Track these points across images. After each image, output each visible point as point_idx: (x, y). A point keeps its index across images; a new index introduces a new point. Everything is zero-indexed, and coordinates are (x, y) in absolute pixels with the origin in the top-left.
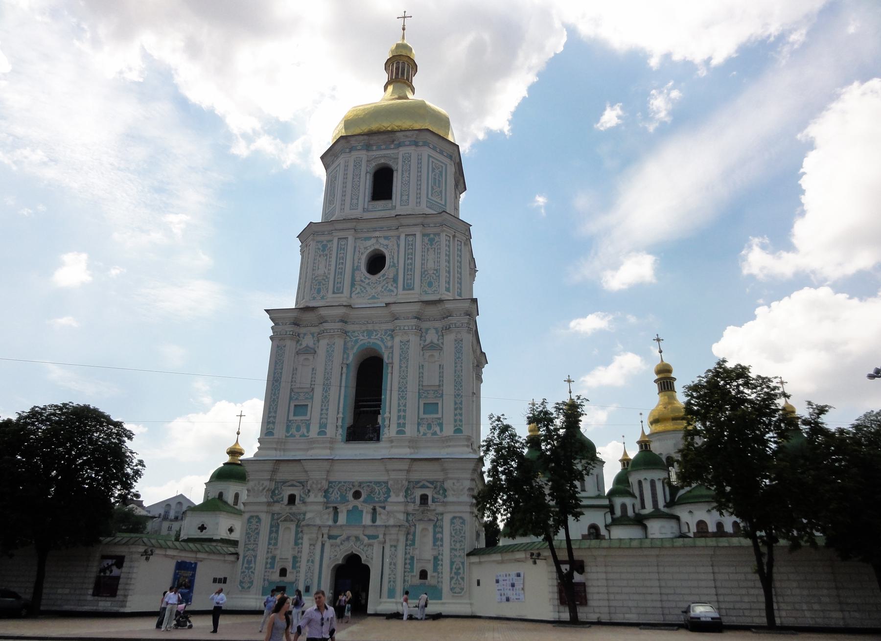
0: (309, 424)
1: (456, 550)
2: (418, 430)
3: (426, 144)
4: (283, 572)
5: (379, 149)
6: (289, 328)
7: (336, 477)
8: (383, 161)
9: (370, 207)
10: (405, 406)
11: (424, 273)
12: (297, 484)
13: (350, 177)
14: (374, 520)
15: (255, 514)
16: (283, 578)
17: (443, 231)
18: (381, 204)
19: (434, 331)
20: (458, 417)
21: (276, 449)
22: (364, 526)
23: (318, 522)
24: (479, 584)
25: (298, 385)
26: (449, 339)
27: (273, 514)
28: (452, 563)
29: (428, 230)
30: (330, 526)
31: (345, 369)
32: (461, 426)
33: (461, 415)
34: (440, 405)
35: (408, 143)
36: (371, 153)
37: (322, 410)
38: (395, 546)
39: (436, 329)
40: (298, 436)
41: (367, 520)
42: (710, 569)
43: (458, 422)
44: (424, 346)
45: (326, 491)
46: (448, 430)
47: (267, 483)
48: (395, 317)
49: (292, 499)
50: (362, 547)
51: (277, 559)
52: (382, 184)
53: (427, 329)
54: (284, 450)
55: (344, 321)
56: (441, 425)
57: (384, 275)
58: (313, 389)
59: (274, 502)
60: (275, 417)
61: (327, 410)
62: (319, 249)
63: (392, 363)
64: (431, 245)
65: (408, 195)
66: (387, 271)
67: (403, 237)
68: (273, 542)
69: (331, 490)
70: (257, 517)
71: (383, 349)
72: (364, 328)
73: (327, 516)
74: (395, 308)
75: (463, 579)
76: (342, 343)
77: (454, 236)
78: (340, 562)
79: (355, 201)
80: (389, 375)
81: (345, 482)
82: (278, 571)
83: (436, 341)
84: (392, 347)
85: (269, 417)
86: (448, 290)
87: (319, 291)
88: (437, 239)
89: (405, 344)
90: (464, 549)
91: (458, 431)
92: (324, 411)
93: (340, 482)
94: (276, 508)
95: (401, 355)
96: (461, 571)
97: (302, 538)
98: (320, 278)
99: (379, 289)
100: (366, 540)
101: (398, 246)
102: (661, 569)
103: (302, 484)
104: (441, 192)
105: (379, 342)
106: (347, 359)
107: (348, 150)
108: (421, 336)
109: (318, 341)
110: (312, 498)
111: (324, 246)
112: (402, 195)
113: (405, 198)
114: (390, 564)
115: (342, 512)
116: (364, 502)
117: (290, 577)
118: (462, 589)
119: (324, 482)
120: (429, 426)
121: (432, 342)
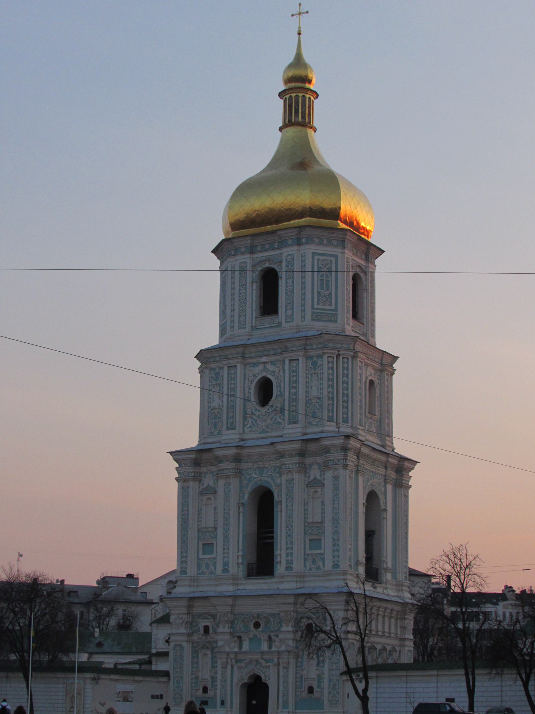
0: (216, 562)
1: (333, 670)
2: (305, 566)
3: (310, 240)
4: (205, 690)
6: (190, 469)
8: (267, 265)
10: (292, 544)
11: (308, 401)
12: (210, 617)
13: (237, 287)
14: (270, 647)
15: (178, 643)
16: (205, 694)
17: (324, 353)
18: (269, 320)
19: (316, 467)
20: (336, 553)
21: (190, 586)
22: (262, 653)
23: (227, 649)
24: (348, 698)
25: (204, 526)
26: (329, 475)
27: (193, 643)
28: (330, 681)
29: (312, 353)
30: (236, 653)
31: (241, 509)
32: (338, 561)
33: (338, 551)
34: (323, 541)
35: (289, 242)
36: (256, 256)
37: (224, 549)
39: (318, 464)
40: (207, 573)
41: (265, 647)
42: (435, 684)
43: (336, 559)
44: (309, 483)
45: (232, 622)
46: (328, 566)
47: (184, 616)
48: (281, 455)
49: (206, 629)
50: (261, 669)
51: (200, 679)
53: (311, 465)
54: (197, 586)
56: (323, 560)
57: (272, 406)
58: (216, 529)
59: (193, 633)
60: (186, 557)
61: (228, 548)
62: (212, 377)
63: (281, 502)
64: (315, 369)
65: (292, 309)
66: (275, 400)
67: (287, 362)
68: (195, 665)
69: (236, 622)
70: (180, 645)
71: (274, 487)
72: (256, 466)
73: (233, 644)
74: (279, 447)
75: (338, 693)
76: (238, 483)
77: (338, 356)
78: (246, 681)
79: (242, 319)
80: (279, 513)
81: (247, 614)
82: (201, 689)
83: (318, 477)
84: (280, 485)
85: (182, 557)
86: (330, 419)
87: (215, 425)
88: (319, 363)
89: (290, 481)
90: (339, 669)
91: (336, 566)
92: (226, 551)
93: (243, 614)
94: (195, 638)
95: (287, 494)
96: (337, 687)
97: (217, 663)
98: (216, 411)
99: (269, 421)
100: (264, 663)
101: (284, 372)
102: (409, 685)
103: (214, 617)
104: (330, 294)
105: (270, 480)
106: (243, 497)
108: (306, 472)
109: (217, 480)
110: (221, 630)
111: (217, 374)
112: (286, 309)
113: (289, 312)
114: (284, 682)
115: (245, 640)
116: (262, 631)
117: (210, 693)
118: (338, 701)
119: (230, 615)
120: (314, 562)
121: (315, 479)
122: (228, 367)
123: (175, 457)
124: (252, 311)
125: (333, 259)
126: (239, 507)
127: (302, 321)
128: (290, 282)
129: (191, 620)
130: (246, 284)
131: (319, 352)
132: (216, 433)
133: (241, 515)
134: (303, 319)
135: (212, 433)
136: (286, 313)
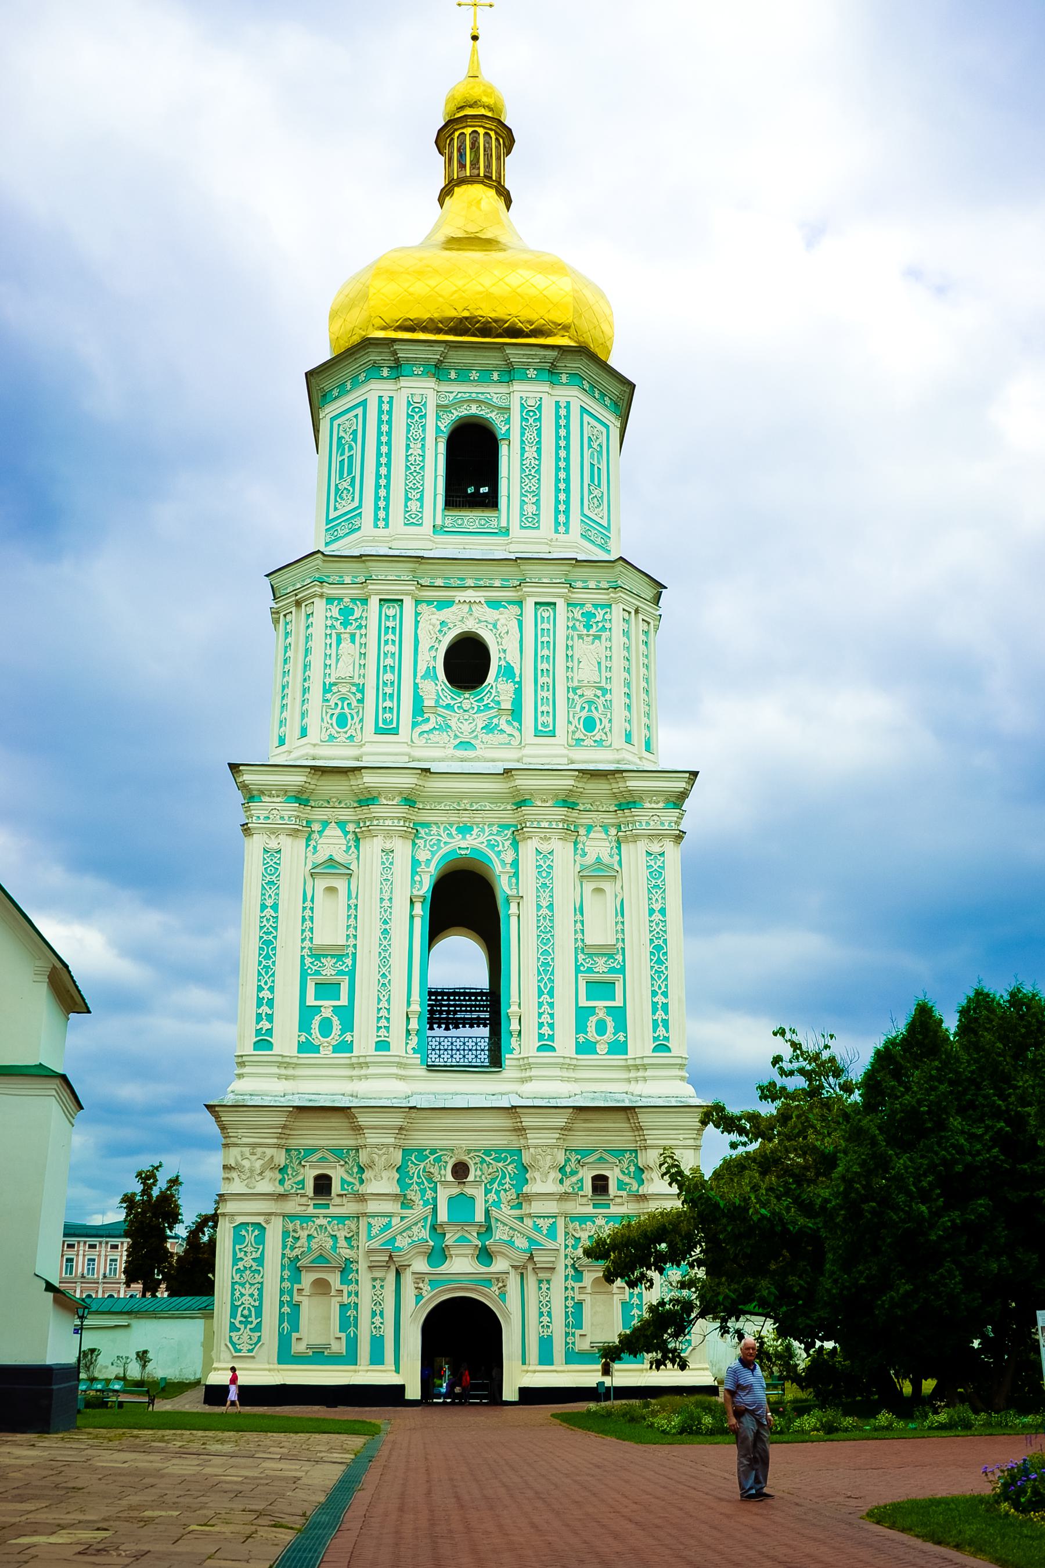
5: (463, 375)
7: (420, 1140)
8: (474, 410)
9: (447, 522)
18: (472, 518)
21: (279, 1077)
36: (444, 387)
38: (548, 1281)
52: (472, 464)
54: (294, 1077)
55: (410, 800)
65: (537, 503)
74: (523, 782)
79: (414, 506)
107: (385, 372)
113: (530, 509)
122: (381, 600)
123: (247, 778)
124: (435, 495)
125: (604, 430)
126: (412, 902)
127: (557, 531)
128: (531, 452)
129: (281, 1158)
130: (423, 439)
131: (602, 597)
132: (343, 738)
133: (418, 922)
134: (562, 529)
135: (332, 737)
136: (522, 508)
